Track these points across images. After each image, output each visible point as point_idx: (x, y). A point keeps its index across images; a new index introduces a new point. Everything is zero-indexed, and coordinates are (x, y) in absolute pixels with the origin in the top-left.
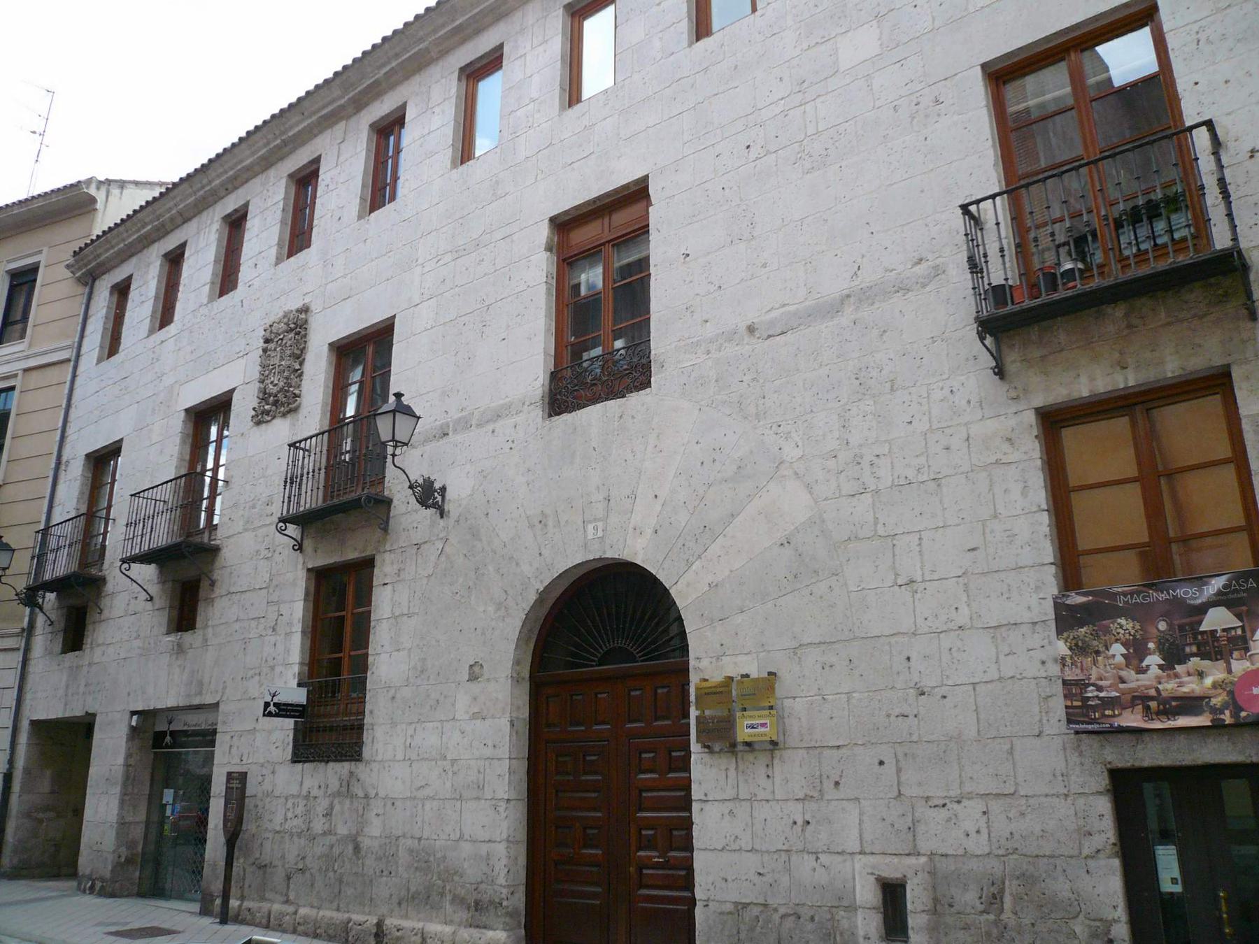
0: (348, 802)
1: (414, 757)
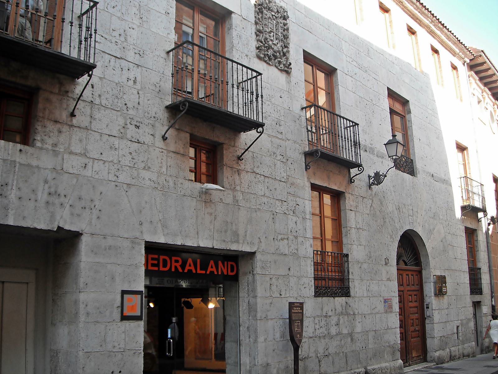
0: (346, 317)
1: (371, 295)
